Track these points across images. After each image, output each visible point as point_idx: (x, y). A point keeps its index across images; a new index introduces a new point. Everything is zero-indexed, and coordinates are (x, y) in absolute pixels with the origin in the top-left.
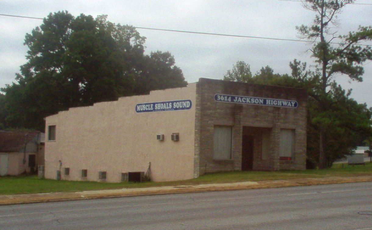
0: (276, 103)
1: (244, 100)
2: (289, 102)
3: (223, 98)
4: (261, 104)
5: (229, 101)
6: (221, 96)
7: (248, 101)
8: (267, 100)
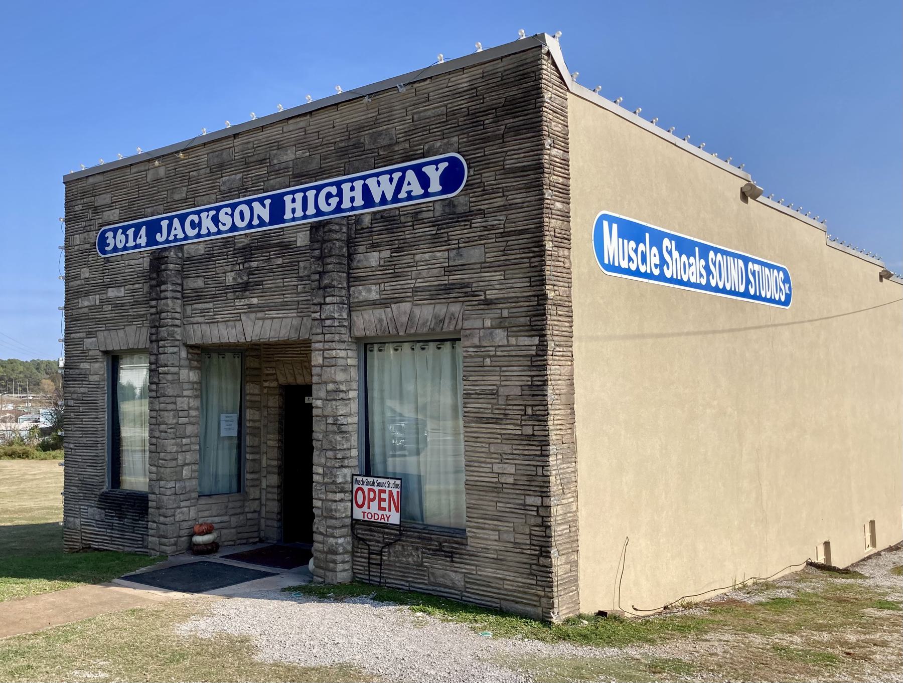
0: (334, 201)
1: (193, 225)
2: (411, 175)
4: (262, 223)
7: (207, 224)
8: (288, 199)
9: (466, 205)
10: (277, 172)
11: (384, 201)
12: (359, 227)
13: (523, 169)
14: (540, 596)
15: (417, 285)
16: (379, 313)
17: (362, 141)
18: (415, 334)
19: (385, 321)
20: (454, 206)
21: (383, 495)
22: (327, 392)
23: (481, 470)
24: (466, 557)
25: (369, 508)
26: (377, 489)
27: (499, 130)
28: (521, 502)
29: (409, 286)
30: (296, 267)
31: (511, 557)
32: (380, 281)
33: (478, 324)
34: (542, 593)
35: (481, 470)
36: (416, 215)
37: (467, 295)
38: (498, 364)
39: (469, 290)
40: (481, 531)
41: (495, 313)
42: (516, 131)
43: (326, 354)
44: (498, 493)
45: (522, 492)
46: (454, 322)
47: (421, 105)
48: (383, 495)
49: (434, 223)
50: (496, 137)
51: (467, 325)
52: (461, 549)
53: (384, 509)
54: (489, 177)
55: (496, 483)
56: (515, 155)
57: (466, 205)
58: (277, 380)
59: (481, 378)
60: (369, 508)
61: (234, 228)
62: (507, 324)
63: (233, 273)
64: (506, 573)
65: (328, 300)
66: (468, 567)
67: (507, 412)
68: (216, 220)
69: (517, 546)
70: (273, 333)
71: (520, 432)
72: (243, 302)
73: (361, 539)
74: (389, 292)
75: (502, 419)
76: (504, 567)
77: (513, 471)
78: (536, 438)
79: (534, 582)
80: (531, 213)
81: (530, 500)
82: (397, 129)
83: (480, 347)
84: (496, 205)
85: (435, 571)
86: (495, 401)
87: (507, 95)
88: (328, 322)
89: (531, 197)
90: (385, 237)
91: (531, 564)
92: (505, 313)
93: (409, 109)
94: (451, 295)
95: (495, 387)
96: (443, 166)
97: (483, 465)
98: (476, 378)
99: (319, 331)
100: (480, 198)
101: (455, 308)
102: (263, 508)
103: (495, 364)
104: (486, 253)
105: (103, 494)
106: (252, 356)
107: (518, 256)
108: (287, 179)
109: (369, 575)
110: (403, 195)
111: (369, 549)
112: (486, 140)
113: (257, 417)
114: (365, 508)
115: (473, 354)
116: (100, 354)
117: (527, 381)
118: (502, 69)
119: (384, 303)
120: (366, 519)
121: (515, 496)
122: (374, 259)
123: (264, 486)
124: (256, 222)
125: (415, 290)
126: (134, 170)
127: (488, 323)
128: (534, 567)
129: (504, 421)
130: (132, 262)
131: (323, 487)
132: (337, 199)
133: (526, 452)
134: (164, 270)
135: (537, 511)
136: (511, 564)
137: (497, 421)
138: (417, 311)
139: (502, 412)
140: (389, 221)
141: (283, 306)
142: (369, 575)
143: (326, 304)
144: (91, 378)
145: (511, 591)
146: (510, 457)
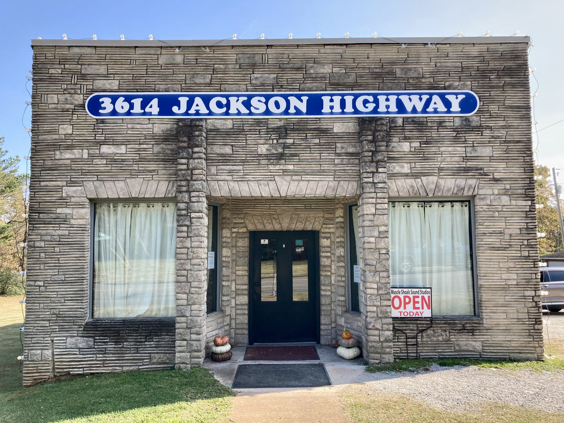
0: (371, 106)
2: (436, 98)
3: (127, 106)
4: (298, 112)
5: (150, 114)
6: (114, 100)
7: (236, 105)
8: (326, 99)
9: (478, 122)
10: (314, 79)
11: (414, 110)
12: (393, 125)
13: (518, 107)
14: (535, 347)
15: (441, 166)
16: (410, 181)
17: (394, 71)
18: (441, 197)
19: (416, 189)
20: (469, 121)
21: (416, 300)
22: (379, 232)
23: (494, 278)
24: (484, 331)
25: (405, 308)
26: (411, 296)
27: (500, 83)
28: (522, 295)
29: (436, 166)
30: (334, 147)
31: (516, 327)
32: (412, 161)
33: (489, 192)
34: (537, 345)
35: (494, 278)
36: (441, 124)
37: (480, 174)
38: (504, 216)
39: (482, 171)
40: (494, 314)
41: (501, 186)
42: (513, 86)
43: (378, 206)
44: (506, 291)
45: (523, 289)
46: (472, 190)
47: (442, 58)
48: (416, 300)
49: (455, 130)
50: (499, 87)
51: (481, 192)
52: (480, 327)
53: (418, 308)
54: (494, 108)
55: (504, 285)
56: (512, 98)
57: (478, 122)
58: (246, 227)
59: (492, 224)
60: (405, 308)
61: (268, 112)
62: (510, 193)
63: (266, 146)
64: (514, 337)
65: (380, 170)
66: (486, 337)
67: (511, 243)
68: (247, 104)
69: (520, 320)
70: (308, 192)
71: (520, 255)
72: (277, 167)
73: (398, 330)
74: (419, 169)
75: (508, 248)
76: (512, 334)
77: (516, 277)
78: (531, 258)
79: (532, 340)
80: (524, 132)
81: (528, 293)
82: (425, 68)
83: (490, 205)
84: (499, 125)
85: (459, 342)
86: (502, 237)
87: (505, 64)
88: (380, 185)
89: (524, 123)
90: (416, 134)
91: (529, 330)
92: (508, 187)
93: (432, 59)
94: (469, 174)
95: (502, 229)
96: (461, 97)
97: (495, 275)
98: (489, 224)
99: (373, 190)
100: (488, 119)
101: (472, 182)
102: (233, 321)
103: (502, 216)
104: (493, 151)
105: (87, 324)
106: (228, 209)
107: (517, 155)
108: (324, 86)
109: (407, 353)
110: (430, 109)
111: (406, 336)
112: (492, 87)
113: (229, 254)
114: (402, 309)
115: (486, 210)
116: (88, 201)
117: (524, 225)
118: (502, 50)
119: (415, 175)
120: (403, 316)
121: (517, 292)
122: (406, 146)
123: (233, 305)
124: (292, 110)
125: (440, 169)
126: (139, 51)
127: (496, 192)
128: (532, 331)
129: (509, 249)
130: (138, 126)
131: (378, 297)
132: (374, 105)
133: (525, 266)
134: (198, 136)
135: (533, 299)
136: (516, 331)
137: (505, 249)
138: (442, 182)
139: (508, 243)
140: (420, 125)
141: (321, 172)
142: (407, 353)
143: (377, 172)
144: (73, 222)
145: (516, 347)
146: (515, 269)
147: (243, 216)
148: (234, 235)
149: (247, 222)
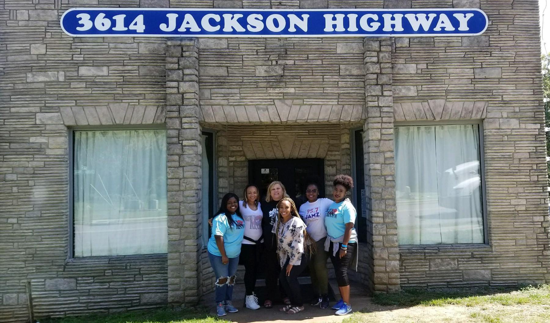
0: (376, 26)
1: (212, 22)
2: (443, 17)
3: (108, 23)
4: (299, 31)
5: (134, 32)
6: (93, 15)
8: (328, 18)
11: (421, 30)
14: (544, 274)
15: (449, 88)
16: (417, 105)
19: (423, 112)
23: (503, 204)
24: (493, 259)
28: (531, 220)
29: (443, 89)
32: (419, 84)
33: (498, 115)
35: (503, 204)
41: (511, 109)
46: (481, 113)
51: (489, 115)
55: (513, 211)
57: (486, 42)
59: (501, 148)
61: (265, 31)
64: (522, 264)
66: (495, 265)
67: (520, 168)
68: (243, 22)
72: (277, 90)
74: (426, 92)
75: (517, 172)
76: (520, 261)
77: (525, 203)
78: (540, 183)
79: (540, 266)
83: (499, 129)
88: (385, 109)
91: (538, 256)
92: (517, 110)
97: (504, 201)
101: (481, 105)
110: (437, 28)
115: (495, 134)
116: (66, 129)
117: (532, 149)
119: (422, 98)
122: (412, 68)
124: (292, 29)
125: (447, 92)
127: (505, 115)
128: (541, 257)
129: (518, 174)
130: (122, 46)
132: (379, 24)
135: (541, 225)
136: (525, 258)
138: (449, 105)
141: (324, 96)
143: (382, 95)
144: (48, 152)
146: (524, 194)
147: (241, 143)
148: (232, 164)
149: (246, 150)
